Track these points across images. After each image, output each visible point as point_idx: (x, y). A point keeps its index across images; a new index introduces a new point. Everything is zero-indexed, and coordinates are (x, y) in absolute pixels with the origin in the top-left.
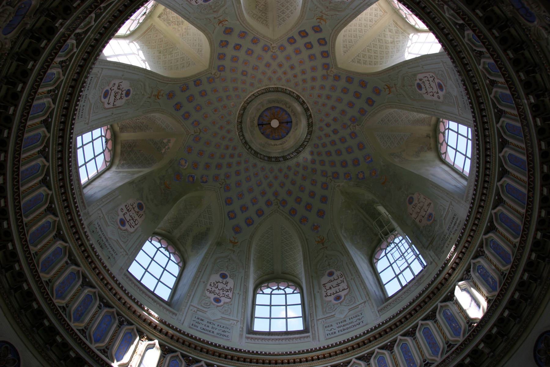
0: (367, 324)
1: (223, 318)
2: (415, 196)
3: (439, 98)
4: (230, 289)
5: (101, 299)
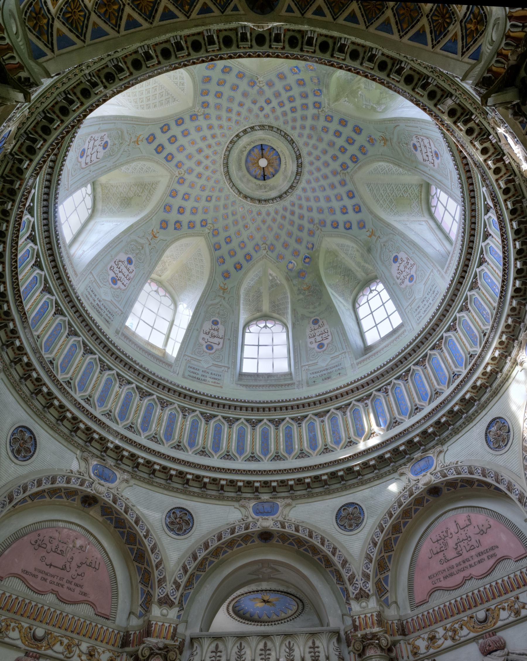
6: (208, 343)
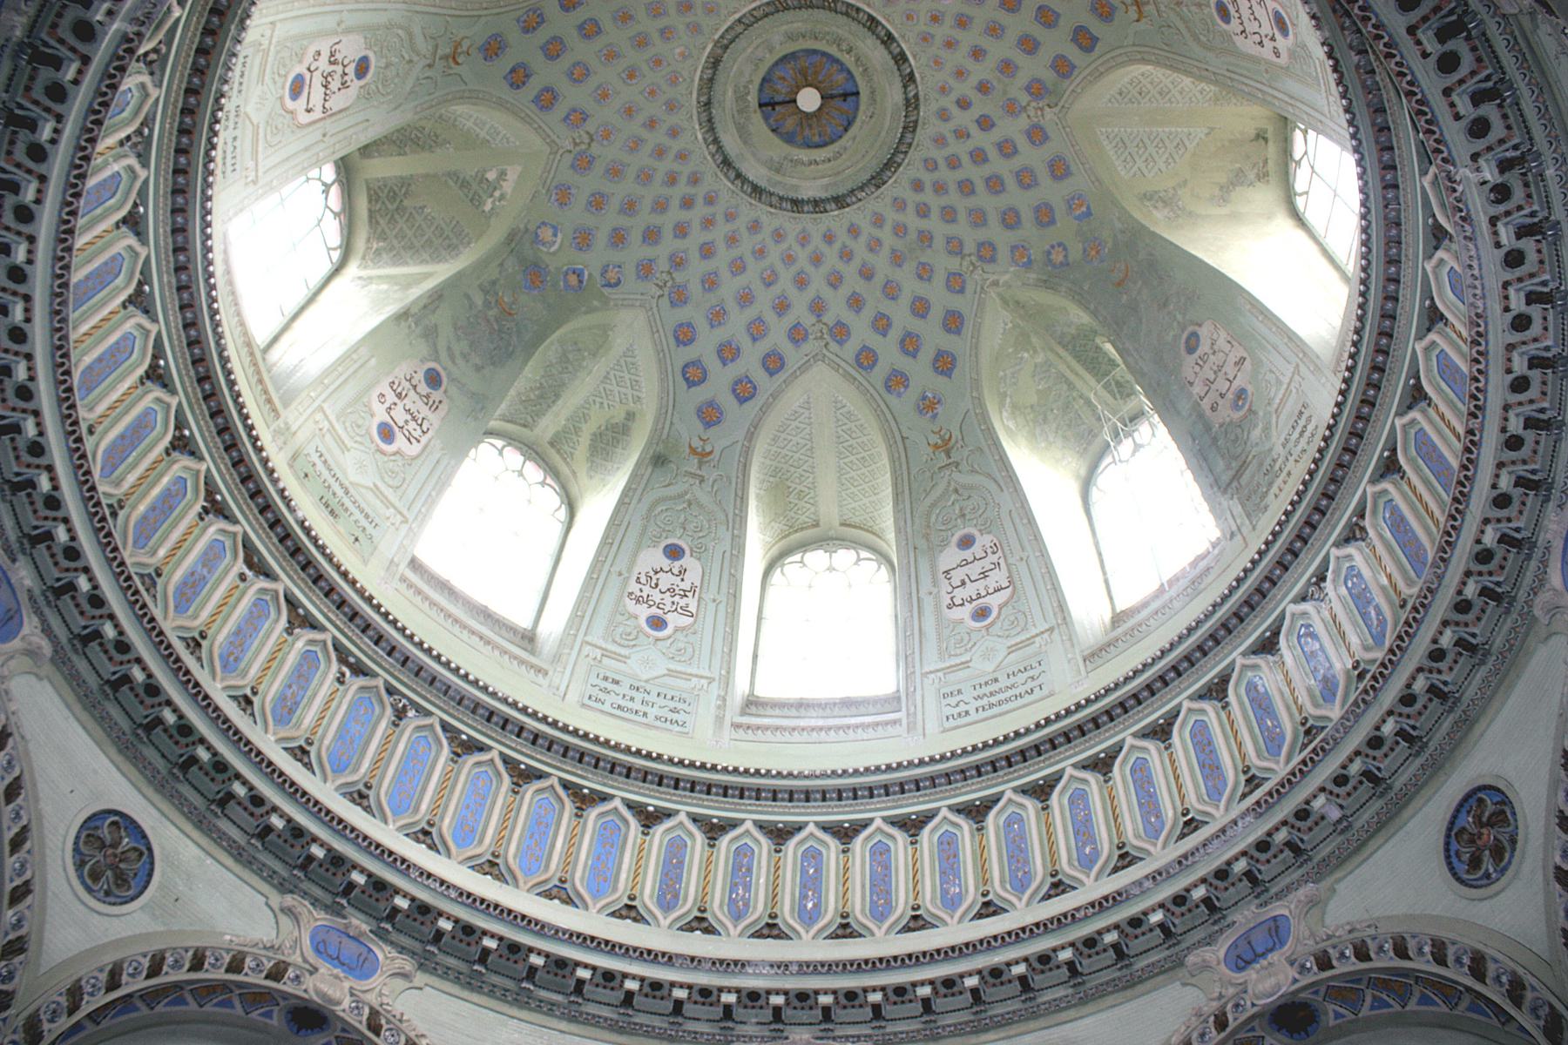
0: (1051, 695)
1: (671, 673)
2: (1204, 332)
3: (1277, 54)
4: (693, 589)
5: (342, 655)
6: (308, 76)
